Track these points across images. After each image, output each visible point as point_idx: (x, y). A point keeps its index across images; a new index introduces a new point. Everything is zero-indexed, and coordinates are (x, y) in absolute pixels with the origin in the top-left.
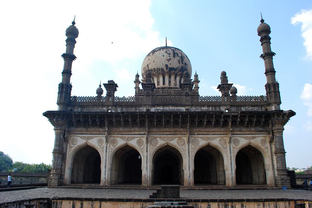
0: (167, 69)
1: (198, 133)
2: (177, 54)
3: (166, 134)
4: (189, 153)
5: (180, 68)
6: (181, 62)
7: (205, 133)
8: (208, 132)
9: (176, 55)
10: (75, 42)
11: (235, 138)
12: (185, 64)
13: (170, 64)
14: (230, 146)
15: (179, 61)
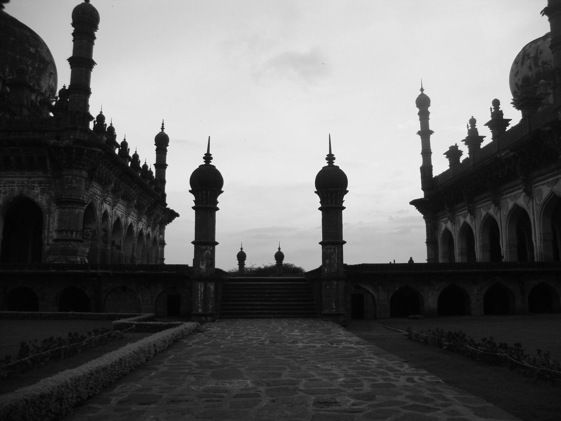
0: (519, 89)
1: (507, 191)
2: (528, 55)
3: (485, 202)
4: (501, 224)
5: (534, 77)
6: (533, 67)
7: (512, 190)
8: (513, 187)
9: (526, 57)
10: (428, 113)
11: (538, 188)
12: (544, 63)
13: (519, 80)
14: (533, 204)
15: (530, 68)
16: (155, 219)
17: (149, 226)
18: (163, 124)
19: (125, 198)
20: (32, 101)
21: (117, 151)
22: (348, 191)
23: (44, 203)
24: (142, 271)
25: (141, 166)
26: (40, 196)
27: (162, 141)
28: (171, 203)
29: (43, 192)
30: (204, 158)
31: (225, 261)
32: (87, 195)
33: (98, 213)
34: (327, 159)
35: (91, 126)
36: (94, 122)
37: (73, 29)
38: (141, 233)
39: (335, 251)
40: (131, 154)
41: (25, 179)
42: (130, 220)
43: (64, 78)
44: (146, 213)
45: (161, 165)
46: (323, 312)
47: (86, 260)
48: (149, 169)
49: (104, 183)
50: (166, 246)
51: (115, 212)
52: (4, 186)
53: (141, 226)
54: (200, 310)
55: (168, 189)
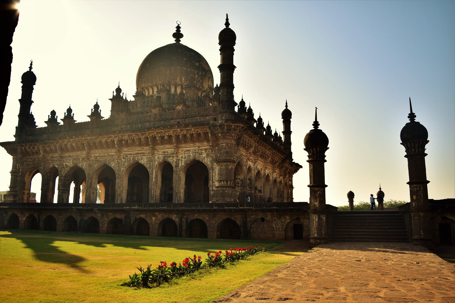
16: (285, 170)
17: (281, 176)
18: (286, 103)
19: (262, 156)
20: (199, 97)
21: (255, 125)
22: (429, 141)
23: (209, 163)
24: (275, 207)
25: (273, 133)
26: (206, 159)
27: (287, 115)
28: (296, 159)
29: (208, 156)
30: (313, 125)
31: (335, 198)
32: (236, 156)
33: (244, 168)
34: (408, 117)
35: (236, 109)
36: (238, 106)
37: (220, 46)
38: (275, 181)
39: (420, 189)
40: (265, 126)
41: (197, 148)
42: (267, 172)
43: (217, 80)
44: (278, 166)
45: (287, 132)
46: (413, 238)
47: (238, 201)
48: (278, 136)
49: (247, 147)
50: (294, 189)
51: (256, 167)
52: (184, 153)
53: (275, 175)
54: (316, 235)
55: (293, 149)
